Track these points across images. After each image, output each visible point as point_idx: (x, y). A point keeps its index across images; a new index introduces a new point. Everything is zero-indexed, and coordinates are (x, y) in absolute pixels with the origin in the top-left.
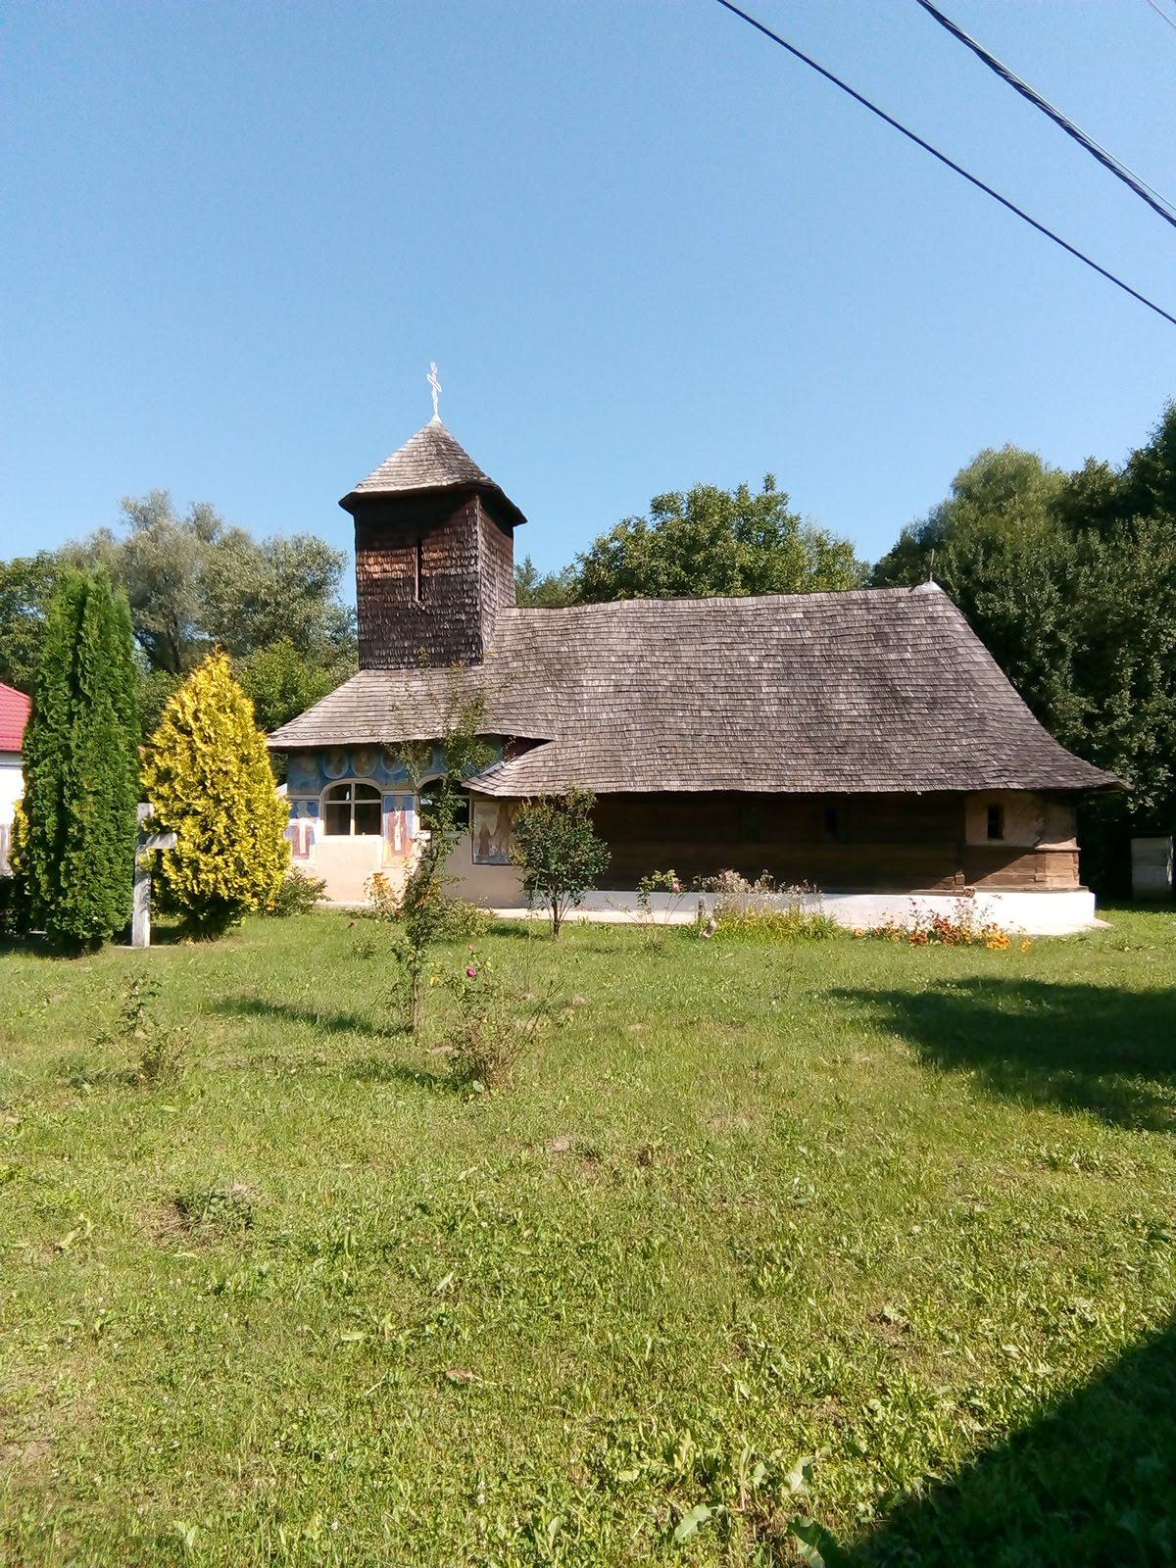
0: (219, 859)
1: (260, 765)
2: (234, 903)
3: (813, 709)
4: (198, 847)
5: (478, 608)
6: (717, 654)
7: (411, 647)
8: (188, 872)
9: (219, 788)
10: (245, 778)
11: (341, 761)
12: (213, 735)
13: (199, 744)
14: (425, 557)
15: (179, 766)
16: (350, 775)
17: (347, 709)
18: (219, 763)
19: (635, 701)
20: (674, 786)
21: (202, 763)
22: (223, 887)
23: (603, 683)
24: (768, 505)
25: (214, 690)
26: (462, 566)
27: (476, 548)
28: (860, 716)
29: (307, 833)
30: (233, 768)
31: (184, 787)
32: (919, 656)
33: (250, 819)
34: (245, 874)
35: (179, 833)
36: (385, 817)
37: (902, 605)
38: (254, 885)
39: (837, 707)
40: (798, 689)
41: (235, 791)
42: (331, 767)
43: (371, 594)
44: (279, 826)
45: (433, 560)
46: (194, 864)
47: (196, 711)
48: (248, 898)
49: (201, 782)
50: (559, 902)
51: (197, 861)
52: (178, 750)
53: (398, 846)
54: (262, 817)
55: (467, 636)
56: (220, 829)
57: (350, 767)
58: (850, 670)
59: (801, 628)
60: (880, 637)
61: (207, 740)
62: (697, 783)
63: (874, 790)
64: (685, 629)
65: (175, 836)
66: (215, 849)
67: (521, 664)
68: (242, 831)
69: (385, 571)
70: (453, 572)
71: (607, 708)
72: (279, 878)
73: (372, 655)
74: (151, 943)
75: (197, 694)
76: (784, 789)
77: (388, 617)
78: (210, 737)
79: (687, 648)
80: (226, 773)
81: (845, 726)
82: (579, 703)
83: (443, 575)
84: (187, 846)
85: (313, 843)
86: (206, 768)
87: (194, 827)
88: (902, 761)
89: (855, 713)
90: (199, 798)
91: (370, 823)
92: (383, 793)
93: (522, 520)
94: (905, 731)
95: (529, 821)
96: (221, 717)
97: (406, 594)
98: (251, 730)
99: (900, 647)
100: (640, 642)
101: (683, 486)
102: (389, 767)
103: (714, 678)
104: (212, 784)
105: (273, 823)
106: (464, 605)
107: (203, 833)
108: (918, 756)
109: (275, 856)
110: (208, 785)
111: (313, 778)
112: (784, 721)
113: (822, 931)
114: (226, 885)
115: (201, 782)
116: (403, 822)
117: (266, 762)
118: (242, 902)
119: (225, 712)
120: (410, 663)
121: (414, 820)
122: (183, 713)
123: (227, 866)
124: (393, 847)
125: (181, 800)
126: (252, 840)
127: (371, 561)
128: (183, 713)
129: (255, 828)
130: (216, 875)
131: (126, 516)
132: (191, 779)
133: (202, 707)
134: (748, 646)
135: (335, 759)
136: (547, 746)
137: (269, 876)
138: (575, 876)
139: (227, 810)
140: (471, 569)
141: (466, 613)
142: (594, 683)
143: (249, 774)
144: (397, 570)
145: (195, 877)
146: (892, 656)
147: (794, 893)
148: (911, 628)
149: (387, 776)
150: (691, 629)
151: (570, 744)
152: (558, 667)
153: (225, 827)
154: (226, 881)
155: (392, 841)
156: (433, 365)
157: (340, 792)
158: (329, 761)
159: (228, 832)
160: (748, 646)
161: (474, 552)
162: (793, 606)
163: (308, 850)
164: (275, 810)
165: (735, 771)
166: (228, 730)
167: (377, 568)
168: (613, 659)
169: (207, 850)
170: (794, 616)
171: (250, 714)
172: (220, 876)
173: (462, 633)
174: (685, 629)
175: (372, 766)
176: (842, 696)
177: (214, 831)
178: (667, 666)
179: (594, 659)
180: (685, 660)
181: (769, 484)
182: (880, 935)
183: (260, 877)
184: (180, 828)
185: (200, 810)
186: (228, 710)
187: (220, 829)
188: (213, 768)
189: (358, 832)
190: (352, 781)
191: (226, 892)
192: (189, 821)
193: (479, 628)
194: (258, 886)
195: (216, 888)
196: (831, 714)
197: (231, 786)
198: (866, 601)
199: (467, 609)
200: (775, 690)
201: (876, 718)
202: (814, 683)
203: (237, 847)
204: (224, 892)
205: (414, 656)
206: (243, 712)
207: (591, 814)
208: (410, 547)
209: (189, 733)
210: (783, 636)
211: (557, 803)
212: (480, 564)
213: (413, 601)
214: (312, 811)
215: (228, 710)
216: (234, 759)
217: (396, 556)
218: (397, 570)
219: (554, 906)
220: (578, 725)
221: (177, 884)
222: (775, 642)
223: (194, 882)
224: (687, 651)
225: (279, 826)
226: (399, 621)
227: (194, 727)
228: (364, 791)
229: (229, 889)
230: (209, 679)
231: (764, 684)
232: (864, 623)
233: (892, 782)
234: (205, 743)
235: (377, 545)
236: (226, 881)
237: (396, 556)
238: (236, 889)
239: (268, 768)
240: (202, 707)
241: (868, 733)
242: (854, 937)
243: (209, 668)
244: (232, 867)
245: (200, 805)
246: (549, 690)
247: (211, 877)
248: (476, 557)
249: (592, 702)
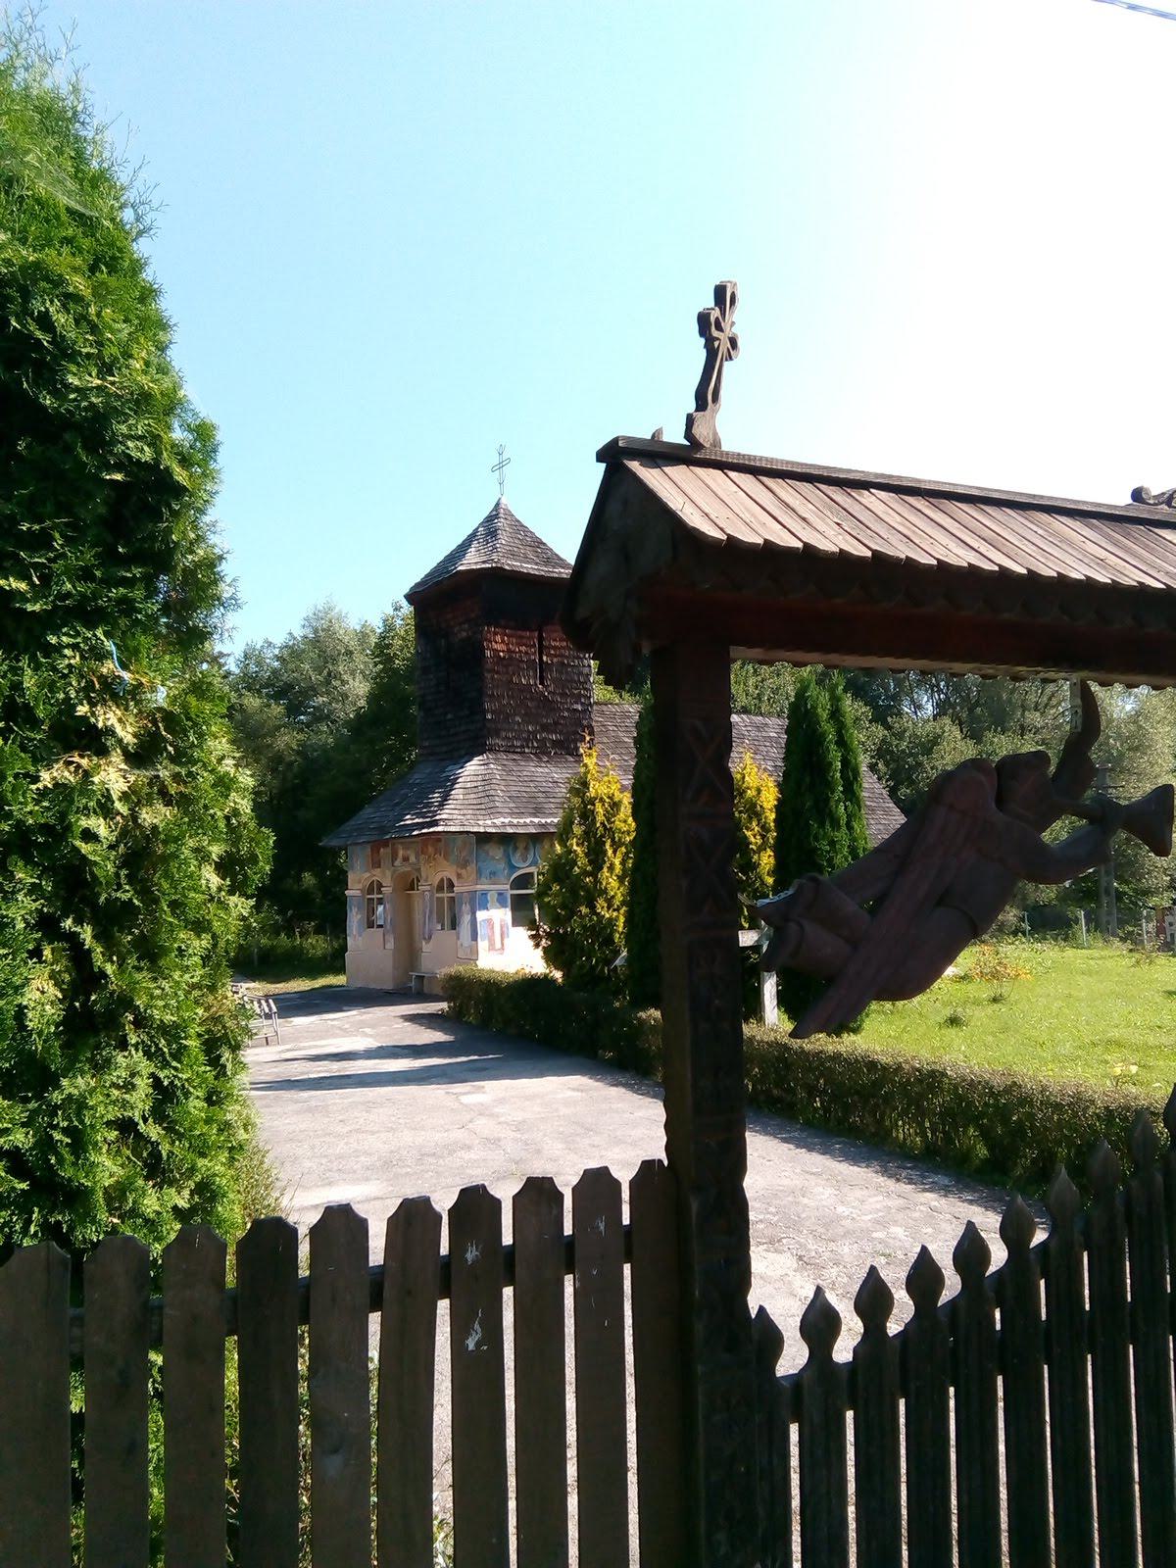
11: (526, 848)
26: (578, 658)
29: (502, 927)
43: (497, 673)
45: (555, 648)
106: (580, 695)
127: (498, 638)
135: (521, 846)
141: (582, 704)
158: (516, 848)
163: (503, 944)
199: (583, 700)
208: (531, 631)
217: (521, 637)
235: (503, 622)
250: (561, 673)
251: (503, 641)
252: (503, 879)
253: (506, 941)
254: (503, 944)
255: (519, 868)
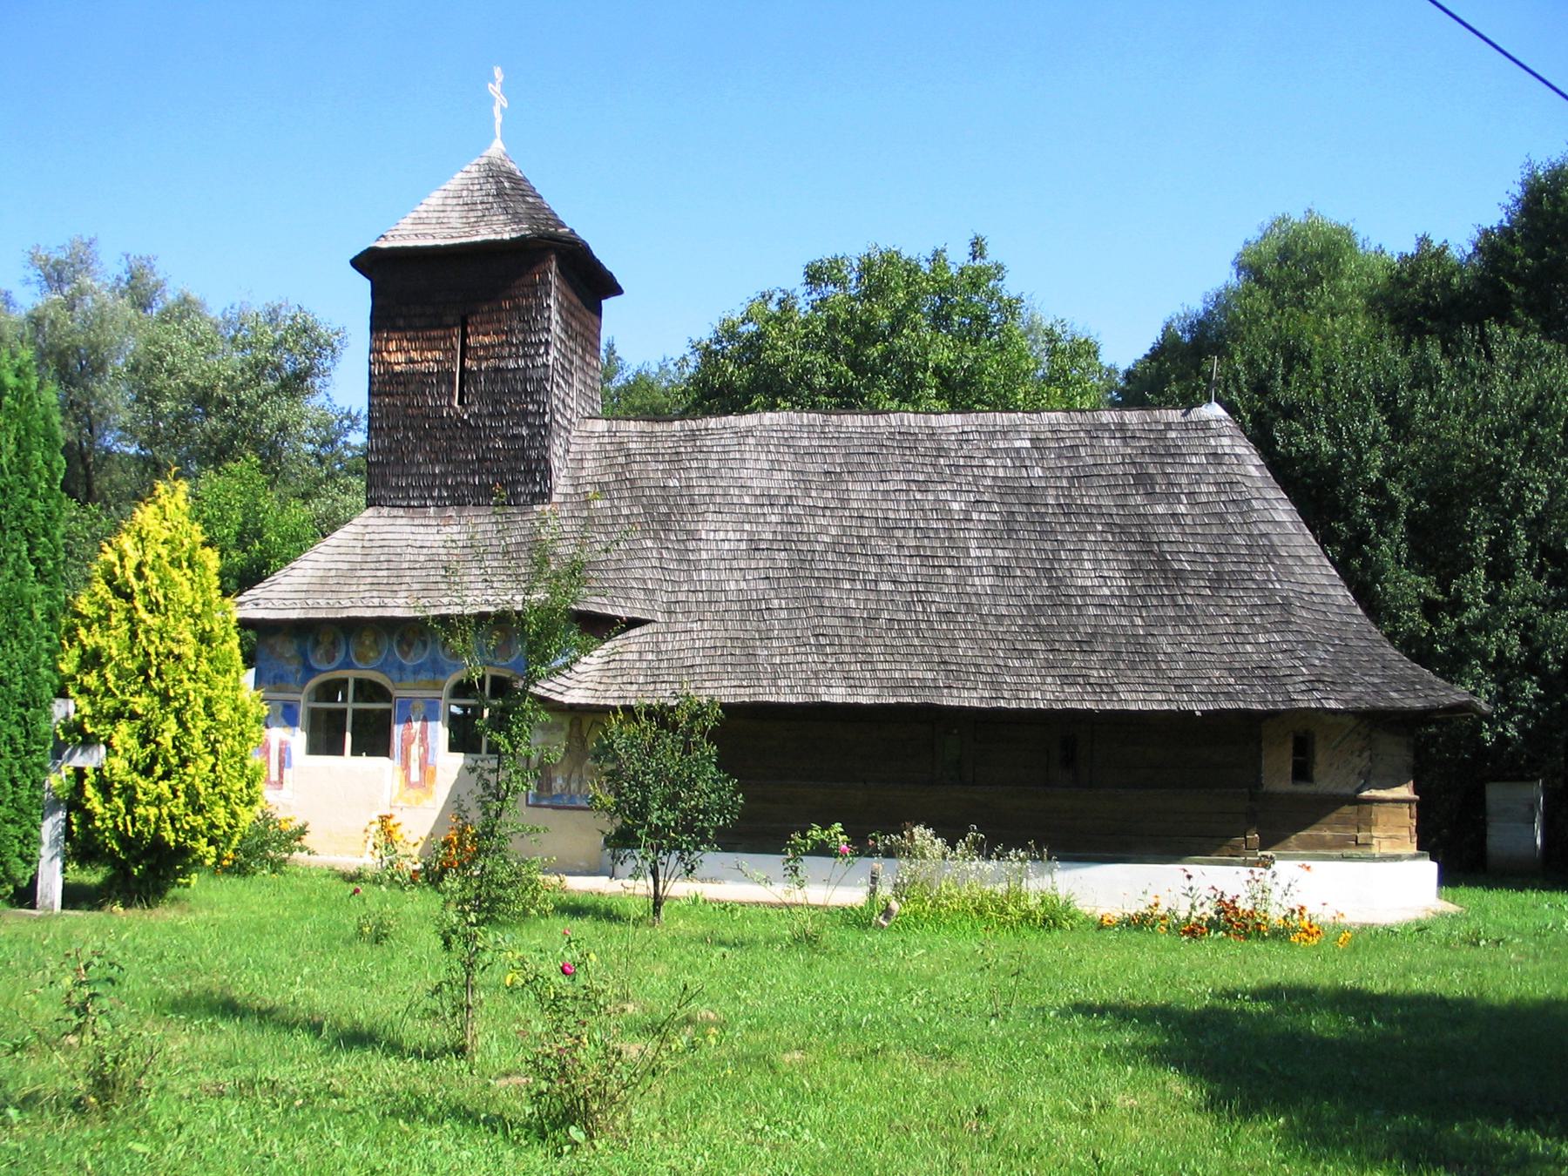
0: (164, 785)
1: (226, 647)
2: (182, 851)
3: (1045, 583)
4: (134, 766)
5: (547, 419)
6: (903, 497)
7: (444, 475)
8: (119, 802)
9: (168, 679)
10: (205, 666)
11: (334, 644)
12: (162, 601)
13: (142, 613)
14: (471, 341)
15: (114, 646)
16: (348, 665)
17: (346, 566)
18: (169, 643)
19: (779, 564)
20: (837, 694)
21: (145, 643)
22: (169, 827)
23: (731, 535)
24: (976, 280)
25: (166, 534)
26: (525, 356)
27: (548, 331)
28: (1113, 596)
29: (281, 751)
30: (188, 651)
31: (119, 677)
32: (1197, 510)
33: (210, 728)
34: (199, 810)
35: (108, 745)
36: (398, 730)
37: (1173, 435)
38: (212, 826)
39: (1080, 582)
40: (1023, 554)
41: (188, 685)
42: (320, 652)
43: (390, 395)
44: (250, 739)
45: (485, 347)
46: (129, 792)
47: (140, 566)
48: (202, 845)
49: (143, 671)
50: (661, 869)
51: (133, 788)
52: (114, 622)
53: (415, 775)
54: (227, 725)
55: (529, 460)
56: (166, 740)
57: (347, 653)
58: (1099, 528)
59: (1028, 463)
60: (1143, 480)
61: (153, 607)
62: (871, 691)
63: (1133, 707)
64: (856, 459)
65: (103, 748)
66: (159, 770)
67: (607, 503)
68: (198, 745)
69: (411, 361)
70: (512, 365)
71: (737, 575)
72: (247, 817)
73: (385, 485)
74: (63, 907)
75: (142, 540)
76: (1002, 704)
77: (412, 428)
78: (157, 603)
79: (858, 487)
80: (178, 658)
81: (1092, 611)
82: (695, 565)
83: (497, 370)
84: (119, 765)
85: (290, 766)
86: (152, 650)
87: (131, 736)
88: (1174, 665)
89: (1107, 592)
90: (139, 693)
91: (374, 740)
92: (396, 693)
93: (617, 290)
94: (1179, 620)
95: (619, 743)
96: (175, 573)
97: (441, 396)
98: (215, 594)
99: (1170, 497)
100: (788, 475)
101: (851, 244)
102: (405, 655)
103: (899, 533)
104: (159, 674)
105: (242, 734)
106: (526, 413)
107: (143, 746)
108: (1197, 657)
109: (243, 784)
110: (152, 673)
111: (293, 667)
112: (1003, 601)
113: (1053, 919)
114: (173, 824)
115: (143, 671)
116: (423, 740)
117: (234, 642)
118: (194, 850)
119: (180, 567)
120: (441, 497)
121: (440, 733)
122: (123, 567)
123: (176, 796)
124: (407, 778)
125: (114, 695)
126: (211, 759)
127: (393, 346)
128: (123, 567)
129: (216, 741)
130: (158, 809)
131: (33, 273)
132: (130, 665)
133: (150, 558)
134: (949, 486)
135: (326, 640)
136: (644, 629)
137: (234, 815)
138: (688, 829)
139: (178, 713)
140: (539, 361)
141: (529, 426)
142: (718, 535)
143: (211, 661)
144: (429, 360)
145: (129, 811)
146: (1160, 509)
147: (1015, 861)
148: (1186, 469)
149: (401, 668)
150: (865, 459)
151: (679, 627)
152: (664, 510)
153: (174, 738)
154: (173, 819)
155: (406, 766)
156: (498, 72)
157: (328, 691)
158: (317, 643)
159: (178, 744)
160: (949, 486)
161: (544, 337)
162: (1016, 429)
163: (281, 776)
164: (245, 715)
165: (929, 675)
166: (184, 594)
167: (401, 357)
168: (747, 500)
169: (147, 772)
170: (1018, 444)
171: (215, 571)
172: (165, 811)
173: (520, 455)
174: (856, 459)
175: (380, 653)
176: (1087, 565)
177: (158, 744)
178: (828, 513)
179: (718, 500)
180: (855, 505)
181: (978, 249)
182: (1139, 923)
183: (220, 815)
184: (110, 737)
185: (140, 711)
186: (185, 564)
187: (166, 740)
188: (161, 649)
189: (356, 751)
190: (350, 675)
191: (173, 836)
192: (124, 727)
193: (547, 449)
194: (217, 827)
195: (158, 828)
196: (1072, 591)
197: (185, 676)
198: (1122, 426)
200: (989, 553)
201: (1135, 600)
202: (1048, 546)
203: (191, 770)
204: (169, 836)
205: (447, 487)
206: (205, 568)
207: (713, 736)
208: (449, 327)
209: (129, 597)
210: (1001, 473)
211: (661, 716)
212: (553, 353)
213: (450, 406)
214: (289, 718)
215: (185, 564)
216: (189, 637)
218: (429, 360)
219: (655, 873)
220: (692, 597)
221: (103, 820)
222: (989, 482)
223: (128, 818)
224: (859, 491)
225: (250, 739)
226: (428, 435)
227: (136, 588)
228: (368, 690)
229: (176, 831)
230: (160, 517)
231: (973, 544)
232: (1119, 459)
233: (1160, 697)
234: (151, 612)
235: (401, 323)
236: (173, 819)
237: (429, 339)
238: (185, 831)
239: (238, 652)
240: (150, 558)
241: (1125, 622)
242: (1101, 927)
243: (161, 502)
244: (182, 799)
245: (140, 703)
246: (649, 543)
247: (153, 811)
248: (547, 343)
249: (714, 565)
250: (494, 382)
251: (399, 350)
252: (293, 686)
253: (286, 771)
254: (281, 776)
255: (321, 672)
